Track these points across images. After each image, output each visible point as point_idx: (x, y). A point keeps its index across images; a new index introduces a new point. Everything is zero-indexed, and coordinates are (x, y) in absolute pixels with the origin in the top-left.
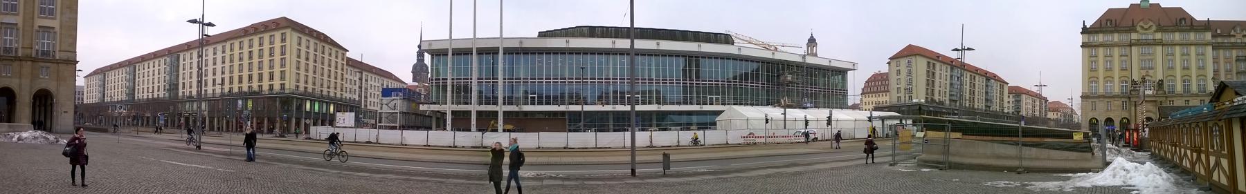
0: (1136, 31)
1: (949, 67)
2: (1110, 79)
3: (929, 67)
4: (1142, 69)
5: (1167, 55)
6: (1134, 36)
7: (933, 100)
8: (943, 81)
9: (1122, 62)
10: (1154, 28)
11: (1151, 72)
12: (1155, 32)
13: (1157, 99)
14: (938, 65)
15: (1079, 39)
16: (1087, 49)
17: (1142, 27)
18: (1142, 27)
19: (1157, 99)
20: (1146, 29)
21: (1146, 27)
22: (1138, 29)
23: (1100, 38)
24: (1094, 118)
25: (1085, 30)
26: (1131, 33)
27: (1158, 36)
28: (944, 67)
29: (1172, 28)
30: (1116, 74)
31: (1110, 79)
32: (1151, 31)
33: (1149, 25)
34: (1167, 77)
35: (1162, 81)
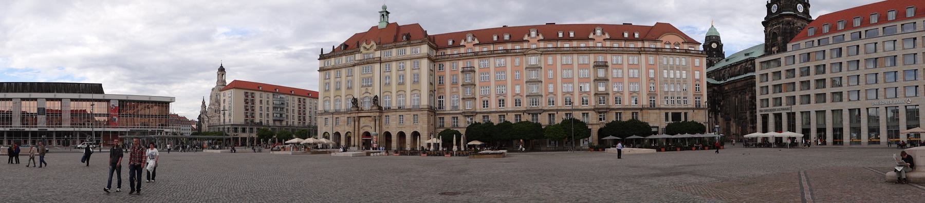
0: (359, 52)
1: (271, 95)
2: (337, 98)
3: (247, 96)
4: (363, 86)
5: (385, 72)
6: (358, 57)
7: (252, 121)
8: (264, 106)
9: (348, 81)
10: (375, 47)
11: (370, 89)
12: (376, 50)
13: (372, 114)
14: (257, 95)
15: (318, 64)
16: (323, 73)
17: (365, 48)
18: (365, 48)
19: (372, 114)
20: (368, 50)
21: (368, 47)
22: (362, 49)
23: (332, 62)
24: (327, 132)
25: (323, 57)
26: (355, 54)
27: (378, 54)
28: (264, 95)
29: (390, 45)
30: (343, 91)
31: (337, 98)
32: (372, 50)
33: (370, 45)
34: (384, 93)
35: (376, 96)
